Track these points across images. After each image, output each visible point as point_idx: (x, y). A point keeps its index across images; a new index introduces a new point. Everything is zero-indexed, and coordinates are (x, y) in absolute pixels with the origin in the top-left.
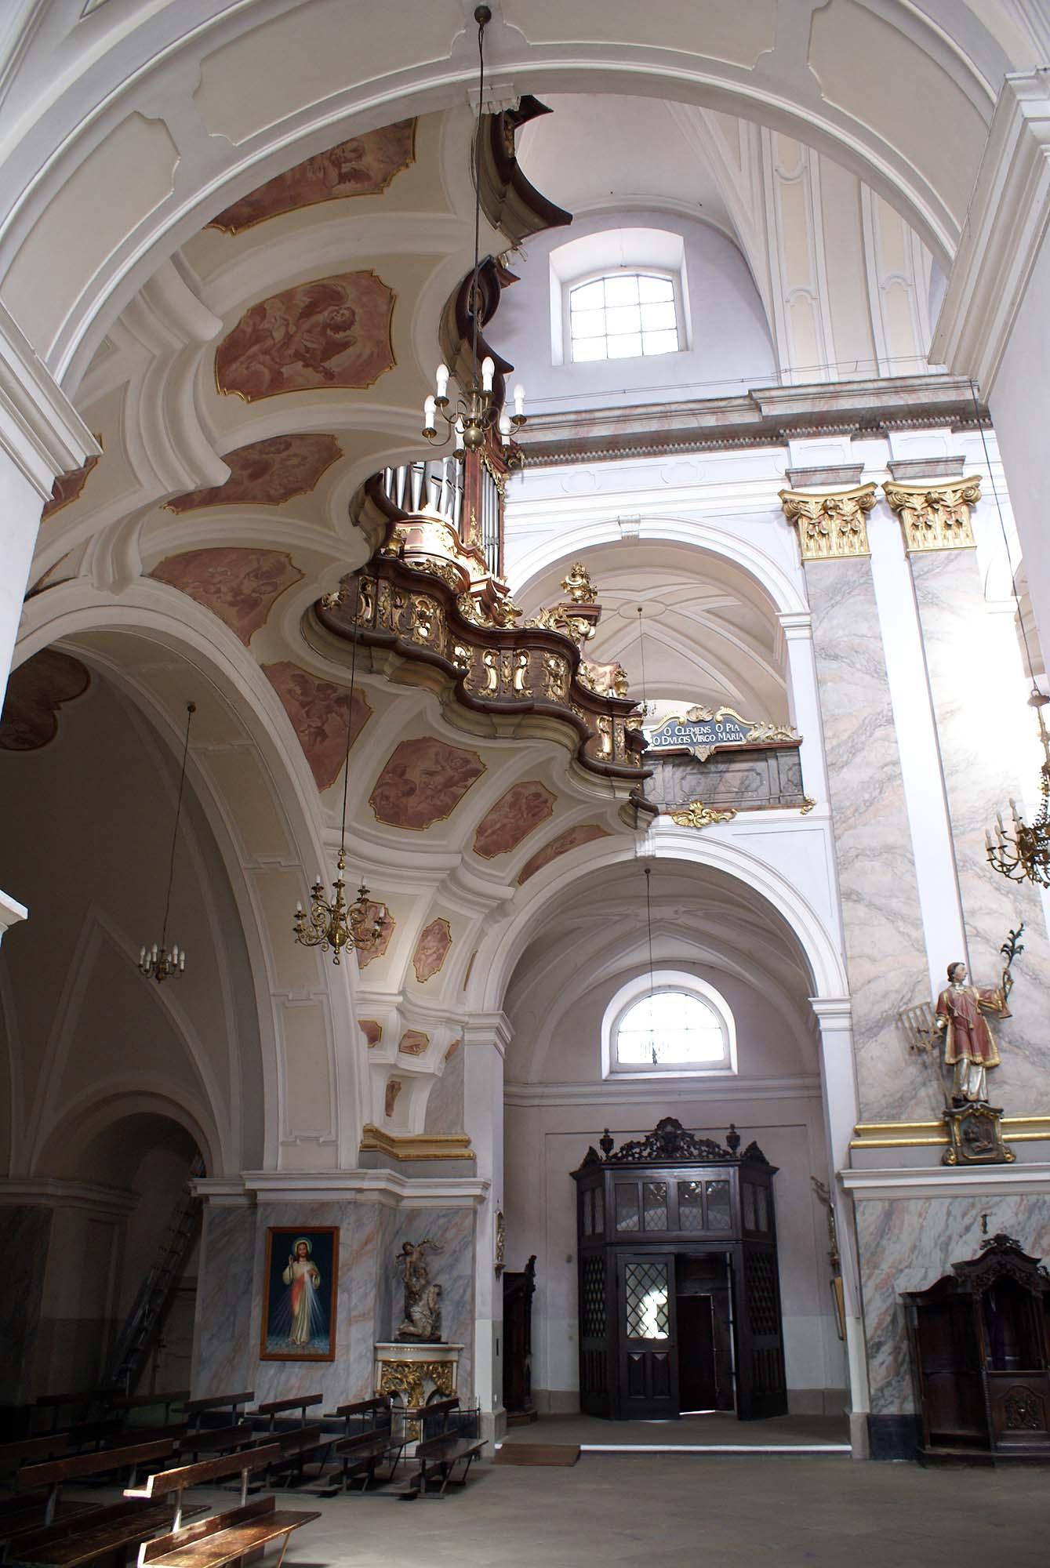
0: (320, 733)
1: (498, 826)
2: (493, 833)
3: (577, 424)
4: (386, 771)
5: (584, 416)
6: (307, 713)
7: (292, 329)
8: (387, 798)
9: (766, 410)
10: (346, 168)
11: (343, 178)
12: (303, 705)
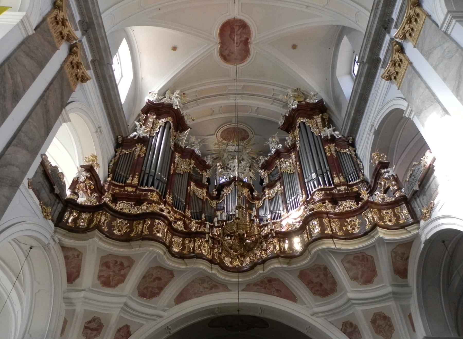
1: (360, 273)
2: (362, 275)
6: (268, 289)
7: (112, 270)
8: (317, 290)
9: (365, 61)
10: (76, 256)
12: (265, 288)
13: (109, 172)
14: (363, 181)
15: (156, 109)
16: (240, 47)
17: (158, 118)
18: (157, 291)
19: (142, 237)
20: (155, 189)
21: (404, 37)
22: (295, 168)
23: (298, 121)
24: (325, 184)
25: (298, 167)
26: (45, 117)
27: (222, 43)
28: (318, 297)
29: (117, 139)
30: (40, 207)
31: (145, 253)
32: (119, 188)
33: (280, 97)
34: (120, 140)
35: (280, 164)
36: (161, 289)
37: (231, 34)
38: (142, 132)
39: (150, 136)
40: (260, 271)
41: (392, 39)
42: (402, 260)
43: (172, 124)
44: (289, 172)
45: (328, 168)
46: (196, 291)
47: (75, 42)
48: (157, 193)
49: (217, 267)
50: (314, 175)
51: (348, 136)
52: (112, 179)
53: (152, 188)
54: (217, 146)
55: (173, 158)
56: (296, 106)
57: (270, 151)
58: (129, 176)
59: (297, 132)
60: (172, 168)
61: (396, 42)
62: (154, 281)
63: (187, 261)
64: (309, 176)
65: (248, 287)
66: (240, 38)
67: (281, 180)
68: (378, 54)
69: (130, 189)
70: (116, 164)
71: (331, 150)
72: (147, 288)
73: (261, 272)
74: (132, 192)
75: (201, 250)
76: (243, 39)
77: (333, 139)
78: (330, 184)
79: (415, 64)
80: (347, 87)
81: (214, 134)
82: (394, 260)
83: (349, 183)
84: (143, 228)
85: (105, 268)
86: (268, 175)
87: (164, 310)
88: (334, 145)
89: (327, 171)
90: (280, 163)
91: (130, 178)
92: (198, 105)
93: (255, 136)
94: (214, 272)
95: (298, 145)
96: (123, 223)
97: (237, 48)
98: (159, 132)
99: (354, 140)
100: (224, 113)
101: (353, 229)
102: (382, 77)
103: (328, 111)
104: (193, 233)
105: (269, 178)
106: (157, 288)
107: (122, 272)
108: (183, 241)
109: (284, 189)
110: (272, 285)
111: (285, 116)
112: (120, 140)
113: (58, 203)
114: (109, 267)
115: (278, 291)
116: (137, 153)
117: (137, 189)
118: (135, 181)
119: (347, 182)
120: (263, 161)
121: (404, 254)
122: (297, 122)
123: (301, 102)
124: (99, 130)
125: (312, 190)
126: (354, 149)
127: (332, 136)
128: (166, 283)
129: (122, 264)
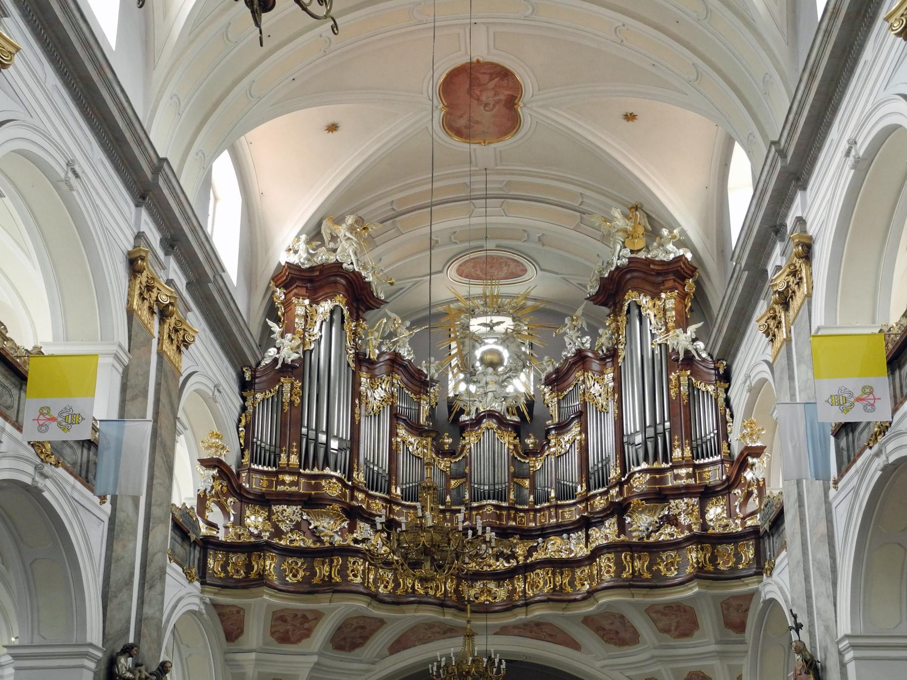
20: (332, 473)
35: (584, 382)
37: (470, 91)
48: (339, 479)
53: (327, 471)
55: (356, 384)
57: (564, 347)
69: (288, 478)
74: (292, 484)
81: (441, 272)
84: (330, 572)
89: (664, 429)
96: (297, 564)
97: (489, 113)
100: (461, 242)
101: (669, 570)
118: (294, 459)
120: (550, 369)
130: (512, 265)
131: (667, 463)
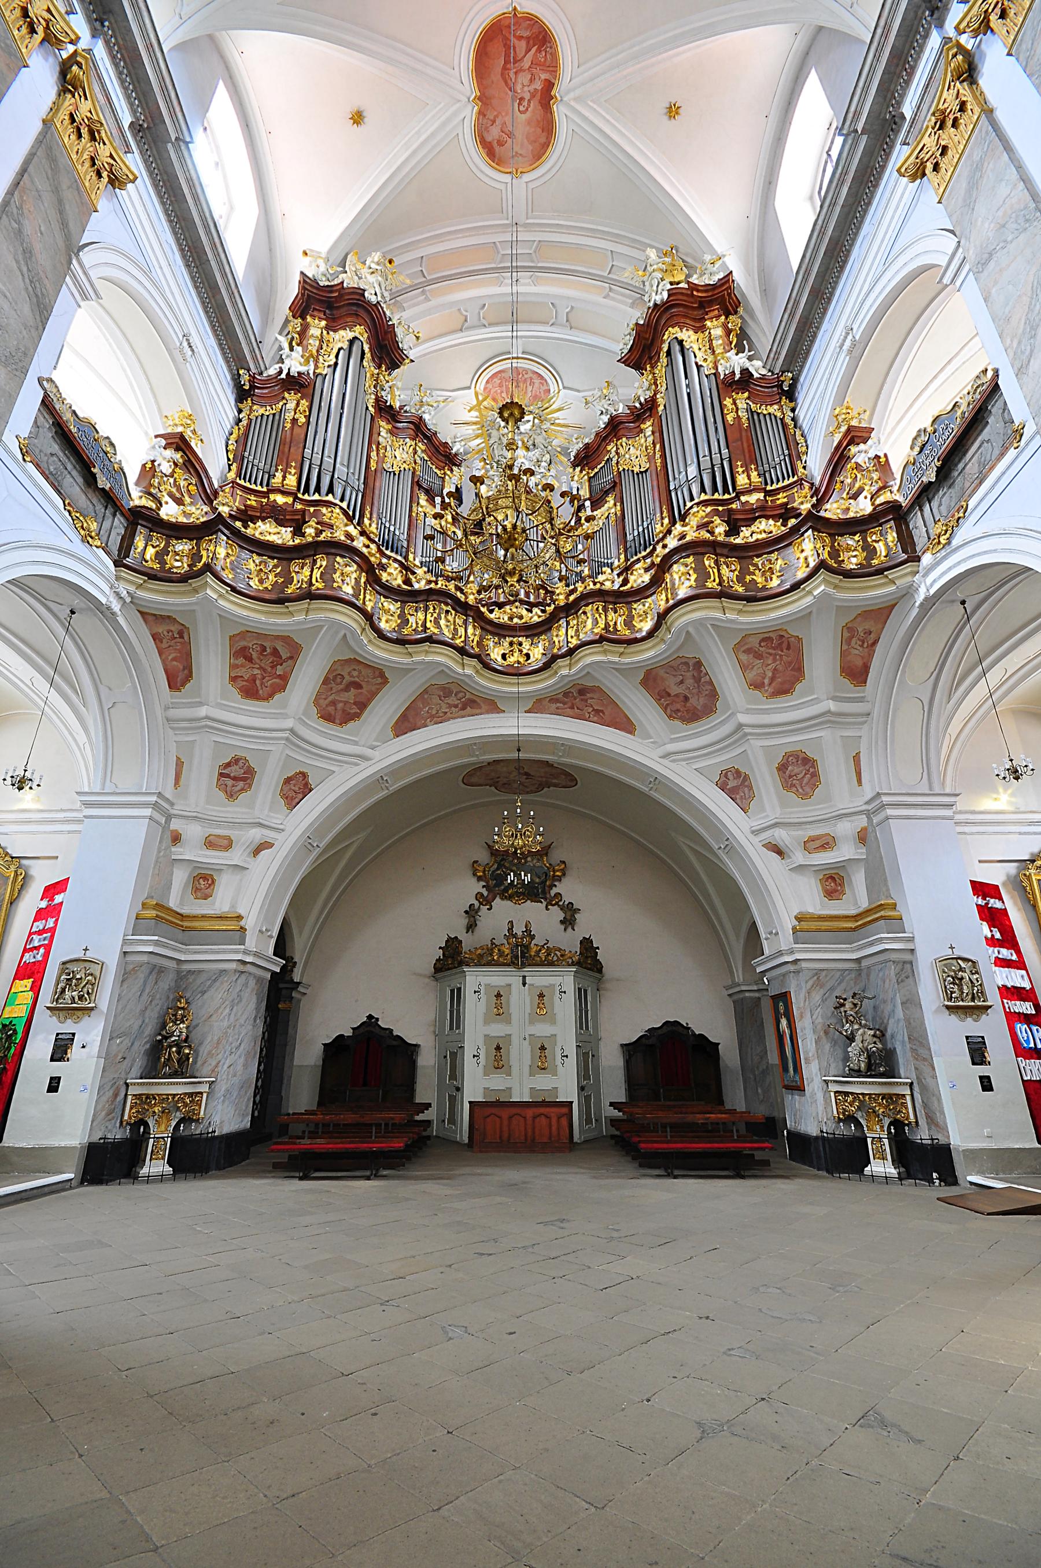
0: (597, 712)
1: (770, 674)
2: (772, 679)
3: (792, 315)
4: (658, 700)
5: (790, 306)
8: (678, 710)
11: (181, 637)
12: (572, 708)
13: (229, 460)
14: (800, 483)
15: (326, 302)
16: (528, 114)
17: (332, 327)
18: (355, 710)
19: (309, 595)
20: (337, 502)
21: (984, 27)
22: (651, 459)
23: (665, 337)
24: (715, 490)
25: (658, 456)
26: (25, 269)
27: (484, 100)
28: (677, 723)
29: (236, 379)
30: (67, 514)
31: (322, 627)
32: (255, 496)
33: (625, 276)
34: (245, 379)
36: (362, 706)
37: (505, 68)
38: (295, 364)
39: (316, 375)
40: (564, 670)
41: (947, 40)
42: (862, 646)
43: (366, 347)
44: (636, 469)
45: (725, 452)
46: (434, 712)
47: (71, 48)
49: (474, 662)
50: (692, 471)
51: (783, 372)
52: (239, 475)
53: (330, 498)
54: (475, 413)
56: (665, 295)
58: (277, 470)
59: (661, 369)
60: (374, 454)
61: (959, 45)
62: (347, 689)
63: (411, 648)
64: (680, 473)
65: (539, 705)
66: (531, 81)
67: (617, 489)
68: (899, 104)
69: (280, 499)
70: (243, 440)
71: (737, 409)
72: (333, 703)
73: (565, 672)
75: (439, 627)
76: (538, 85)
77: (744, 381)
78: (726, 490)
79: (1000, 115)
80: (797, 221)
81: (469, 388)
82: (845, 647)
83: (769, 488)
84: (311, 576)
85: (241, 661)
86: (590, 478)
87: (373, 748)
88: (746, 394)
89: (722, 460)
90: (618, 449)
91: (279, 475)
92: (427, 300)
93: (563, 391)
94: (468, 671)
95: (660, 401)
97: (523, 117)
98: (336, 364)
99: (795, 380)
102: (898, 171)
103: (741, 310)
104: (420, 592)
105: (590, 486)
106: (355, 703)
107: (279, 670)
108: (402, 608)
109: (623, 510)
110: (586, 701)
111: (637, 324)
112: (245, 379)
113: (114, 515)
114: (250, 659)
115: (597, 712)
116: (289, 416)
117: (296, 498)
118: (291, 481)
119: (766, 484)
121: (870, 633)
122: (663, 342)
123: (678, 283)
124: (185, 344)
125: (685, 505)
126: (792, 405)
127: (745, 372)
128: (374, 694)
129: (275, 652)
130: (537, 381)
131: (729, 493)
